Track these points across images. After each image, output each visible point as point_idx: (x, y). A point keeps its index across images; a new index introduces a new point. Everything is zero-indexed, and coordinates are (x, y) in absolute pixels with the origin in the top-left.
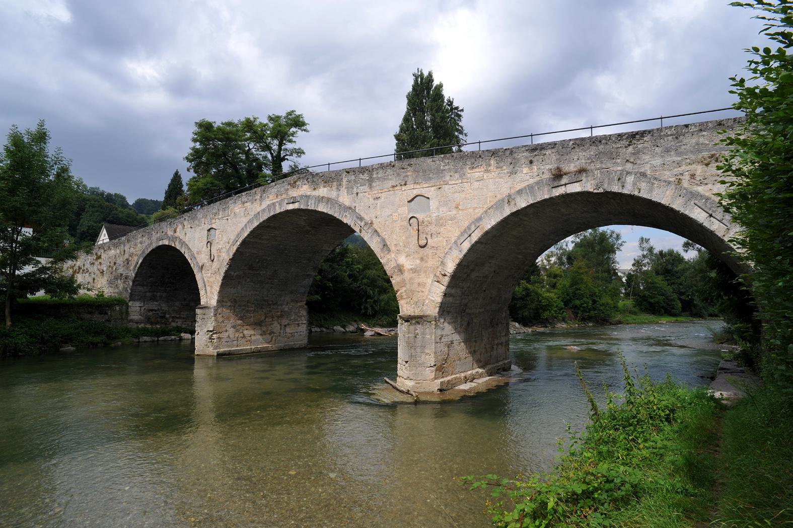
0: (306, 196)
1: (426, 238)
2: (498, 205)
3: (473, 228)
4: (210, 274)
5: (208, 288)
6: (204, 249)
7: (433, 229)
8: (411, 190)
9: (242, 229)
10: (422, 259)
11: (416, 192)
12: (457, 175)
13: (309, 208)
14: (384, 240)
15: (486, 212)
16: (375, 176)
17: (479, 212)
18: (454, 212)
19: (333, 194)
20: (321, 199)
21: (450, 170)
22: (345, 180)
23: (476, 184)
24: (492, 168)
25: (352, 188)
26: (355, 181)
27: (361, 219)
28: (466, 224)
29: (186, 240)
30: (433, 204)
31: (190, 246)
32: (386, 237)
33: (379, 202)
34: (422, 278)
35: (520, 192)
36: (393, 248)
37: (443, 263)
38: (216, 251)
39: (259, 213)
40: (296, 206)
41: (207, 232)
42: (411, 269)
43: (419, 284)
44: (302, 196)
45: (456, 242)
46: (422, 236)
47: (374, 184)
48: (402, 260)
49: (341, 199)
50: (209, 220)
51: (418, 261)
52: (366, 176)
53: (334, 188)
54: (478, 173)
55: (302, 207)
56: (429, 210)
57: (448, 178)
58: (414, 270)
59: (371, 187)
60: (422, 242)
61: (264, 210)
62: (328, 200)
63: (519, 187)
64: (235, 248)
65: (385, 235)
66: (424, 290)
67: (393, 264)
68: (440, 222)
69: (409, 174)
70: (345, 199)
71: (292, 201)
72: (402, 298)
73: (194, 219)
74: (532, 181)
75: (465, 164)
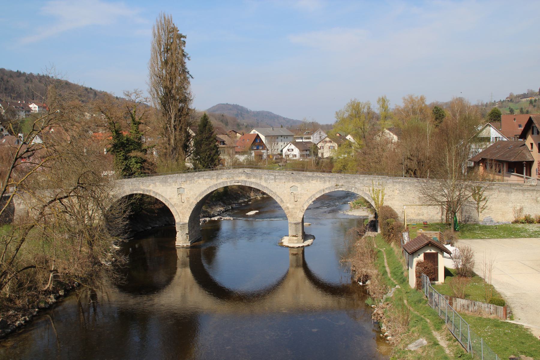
0: (245, 181)
2: (320, 191)
3: (313, 197)
4: (181, 209)
5: (181, 215)
6: (175, 197)
7: (299, 196)
8: (291, 184)
9: (206, 190)
10: (295, 205)
11: (293, 185)
12: (307, 182)
13: (247, 185)
14: (281, 199)
15: (317, 193)
16: (277, 177)
17: (314, 193)
18: (306, 192)
19: (258, 181)
20: (252, 183)
21: (305, 180)
22: (263, 178)
23: (313, 185)
24: (318, 181)
25: (267, 180)
26: (268, 178)
27: (272, 191)
28: (310, 196)
29: (159, 191)
30: (299, 189)
31: (163, 195)
33: (279, 186)
34: (296, 210)
35: (326, 188)
36: (284, 201)
37: (303, 207)
38: (185, 199)
39: (217, 184)
40: (240, 184)
41: (177, 189)
43: (295, 212)
44: (242, 181)
45: (307, 201)
46: (296, 198)
47: (276, 180)
48: (288, 205)
49: (262, 184)
50: (179, 184)
51: (294, 206)
52: (273, 177)
53: (259, 179)
54: (314, 182)
55: (243, 185)
56: (298, 191)
57: (304, 182)
58: (293, 208)
59: (275, 181)
60: (296, 200)
61: (220, 184)
62: (256, 183)
63: (326, 187)
64: (201, 198)
65: (281, 197)
67: (285, 206)
68: (301, 194)
70: (263, 183)
71: (237, 182)
72: (289, 216)
73: (166, 182)
74: (329, 186)
75: (310, 179)
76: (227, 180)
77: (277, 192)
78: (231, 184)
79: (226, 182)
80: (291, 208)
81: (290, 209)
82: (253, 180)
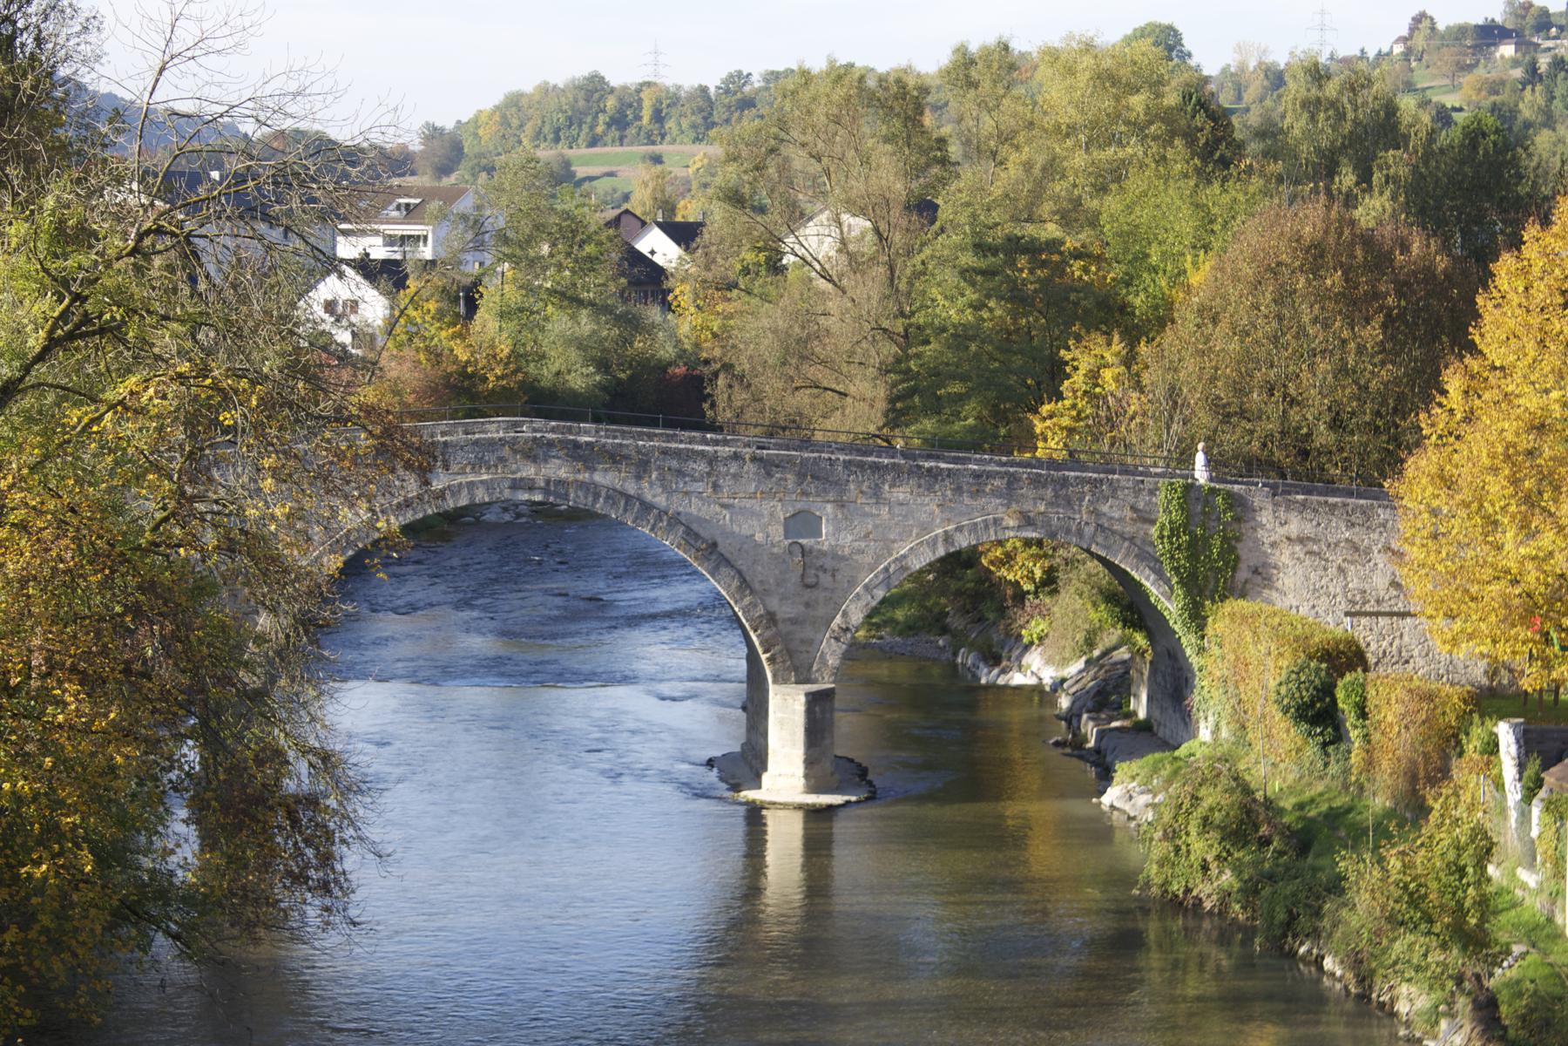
1: (817, 576)
2: (933, 544)
10: (807, 605)
11: (799, 506)
18: (863, 544)
32: (744, 568)
34: (808, 632)
37: (845, 614)
42: (789, 619)
43: (802, 641)
49: (648, 497)
51: (802, 608)
54: (901, 493)
58: (794, 621)
59: (716, 487)
60: (811, 580)
66: (810, 649)
69: (789, 476)
76: (471, 478)
77: (719, 540)
78: (490, 495)
79: (471, 485)
80: (784, 620)
81: (781, 626)
82: (604, 477)
